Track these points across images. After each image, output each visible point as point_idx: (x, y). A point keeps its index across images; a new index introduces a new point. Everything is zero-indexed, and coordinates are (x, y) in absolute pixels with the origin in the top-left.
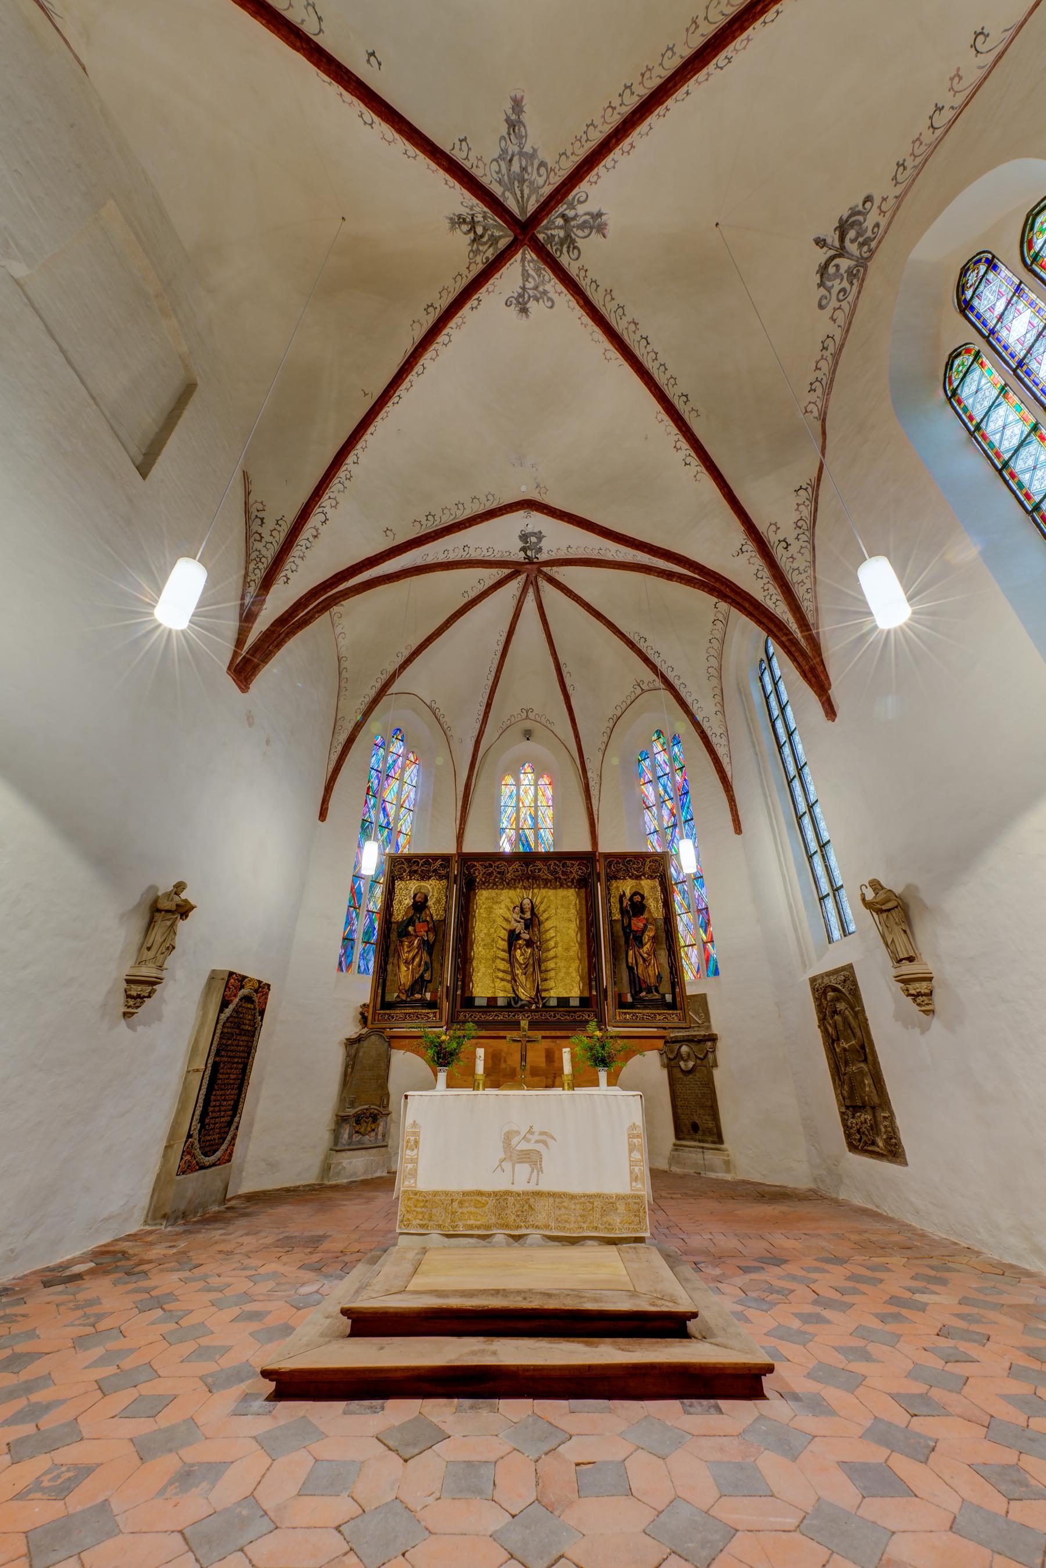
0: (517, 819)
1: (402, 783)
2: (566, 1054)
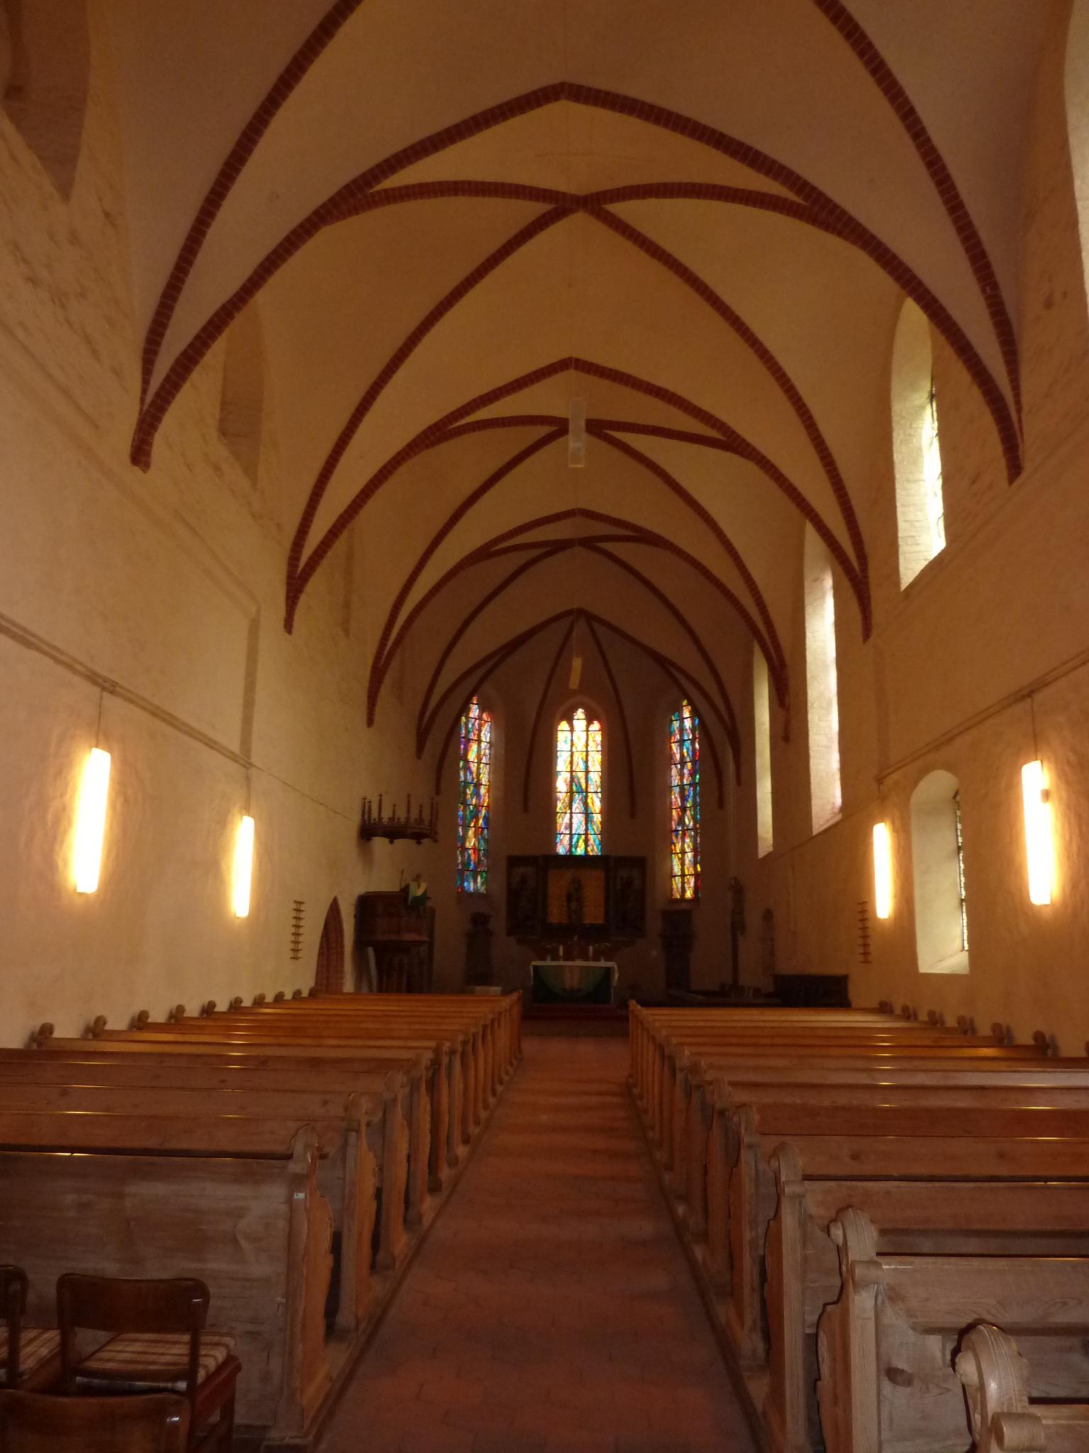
0: (571, 763)
1: (479, 741)
2: (591, 948)
